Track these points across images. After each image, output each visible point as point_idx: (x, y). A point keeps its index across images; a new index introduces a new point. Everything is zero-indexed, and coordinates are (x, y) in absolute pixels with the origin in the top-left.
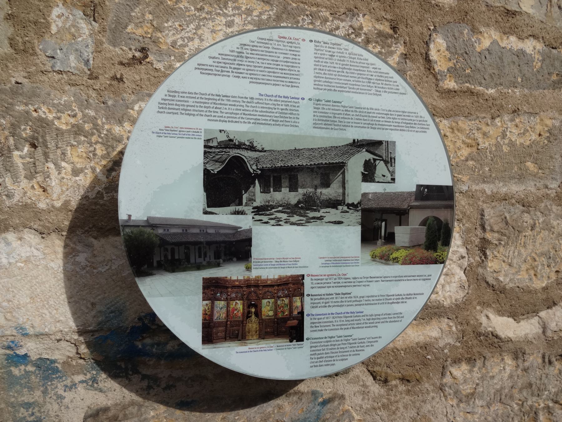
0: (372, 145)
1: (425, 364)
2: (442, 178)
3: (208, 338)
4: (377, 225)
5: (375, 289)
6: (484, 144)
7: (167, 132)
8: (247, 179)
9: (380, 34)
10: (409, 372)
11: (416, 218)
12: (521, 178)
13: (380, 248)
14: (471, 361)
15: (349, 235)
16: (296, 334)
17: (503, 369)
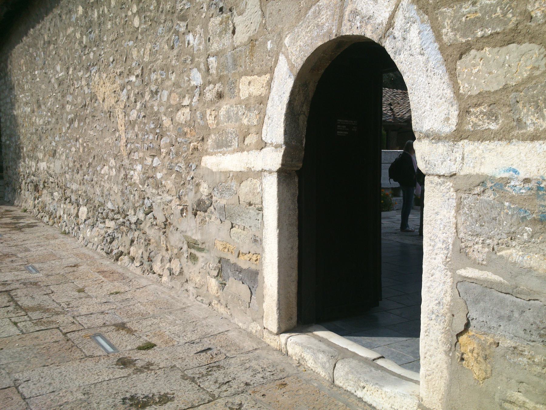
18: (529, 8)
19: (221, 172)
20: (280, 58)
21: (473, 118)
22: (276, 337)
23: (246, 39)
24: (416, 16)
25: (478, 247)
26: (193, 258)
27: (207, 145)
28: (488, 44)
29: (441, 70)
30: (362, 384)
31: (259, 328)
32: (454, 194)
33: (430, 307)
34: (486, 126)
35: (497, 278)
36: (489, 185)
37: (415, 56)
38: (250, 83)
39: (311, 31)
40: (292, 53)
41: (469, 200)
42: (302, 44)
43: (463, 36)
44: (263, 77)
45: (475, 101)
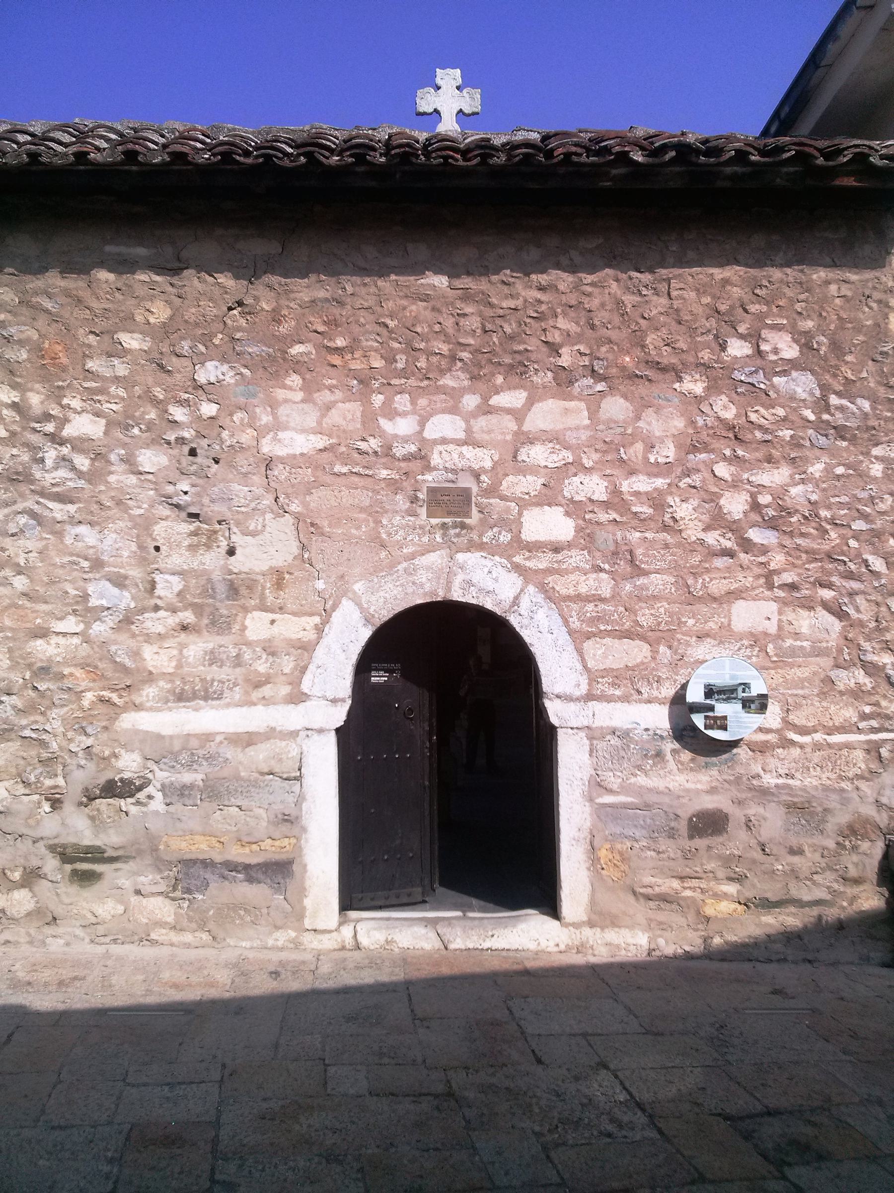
0: (744, 684)
1: (767, 747)
2: (764, 691)
3: (705, 729)
4: (746, 704)
5: (746, 720)
6: (788, 677)
7: (696, 683)
8: (714, 693)
9: (751, 645)
10: (762, 749)
11: (757, 702)
12: (802, 688)
13: (747, 710)
14: (783, 748)
15: (739, 706)
16: (726, 729)
17: (796, 752)
18: (638, 619)
19: (189, 735)
20: (344, 601)
21: (599, 686)
22: (335, 933)
23: (265, 568)
24: (543, 603)
25: (612, 779)
26: (86, 878)
27: (142, 696)
28: (609, 636)
29: (571, 648)
30: (490, 933)
31: (293, 934)
32: (588, 742)
33: (571, 836)
34: (611, 692)
35: (630, 799)
36: (617, 733)
37: (542, 633)
38: (273, 622)
39: (402, 585)
40: (369, 601)
41: (600, 745)
42: (387, 595)
43: (588, 626)
44: (308, 619)
45: (601, 674)
